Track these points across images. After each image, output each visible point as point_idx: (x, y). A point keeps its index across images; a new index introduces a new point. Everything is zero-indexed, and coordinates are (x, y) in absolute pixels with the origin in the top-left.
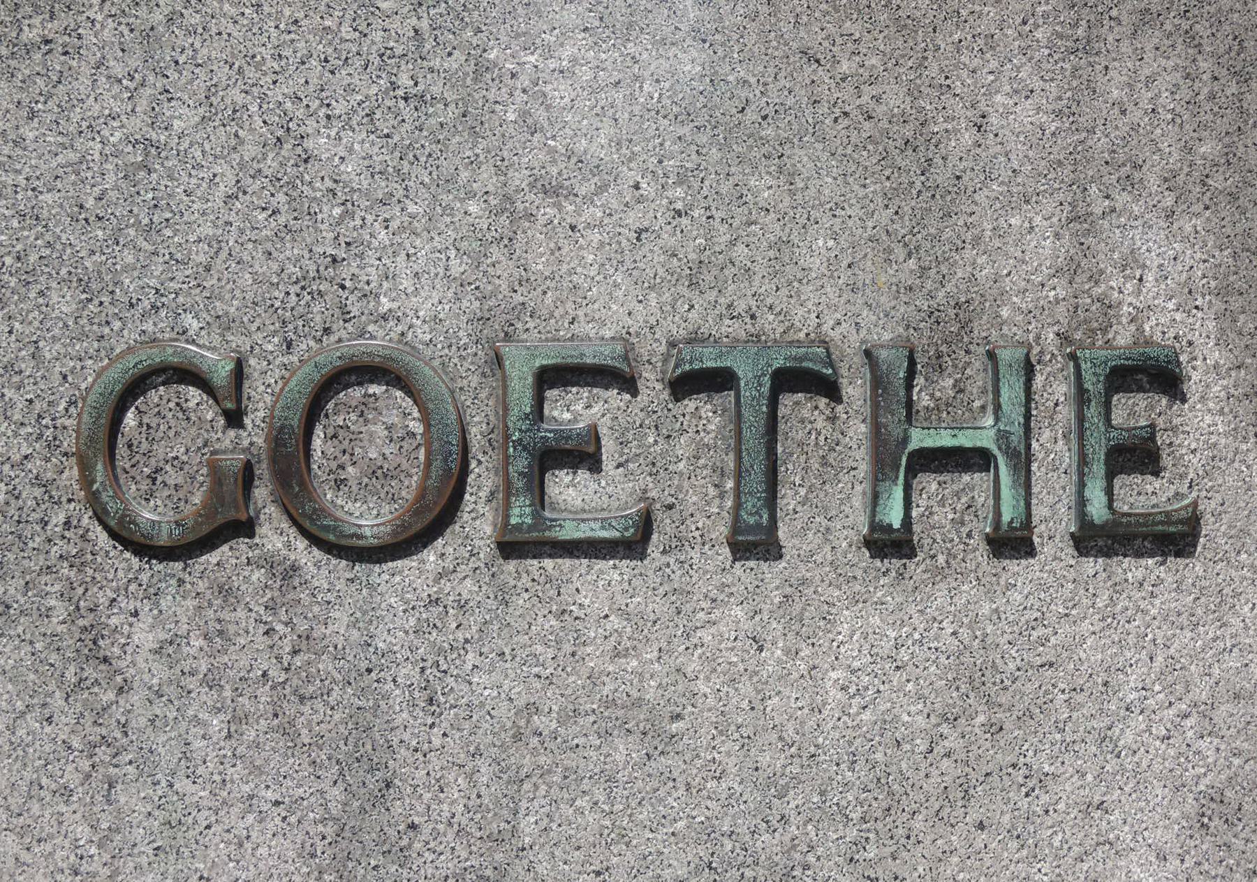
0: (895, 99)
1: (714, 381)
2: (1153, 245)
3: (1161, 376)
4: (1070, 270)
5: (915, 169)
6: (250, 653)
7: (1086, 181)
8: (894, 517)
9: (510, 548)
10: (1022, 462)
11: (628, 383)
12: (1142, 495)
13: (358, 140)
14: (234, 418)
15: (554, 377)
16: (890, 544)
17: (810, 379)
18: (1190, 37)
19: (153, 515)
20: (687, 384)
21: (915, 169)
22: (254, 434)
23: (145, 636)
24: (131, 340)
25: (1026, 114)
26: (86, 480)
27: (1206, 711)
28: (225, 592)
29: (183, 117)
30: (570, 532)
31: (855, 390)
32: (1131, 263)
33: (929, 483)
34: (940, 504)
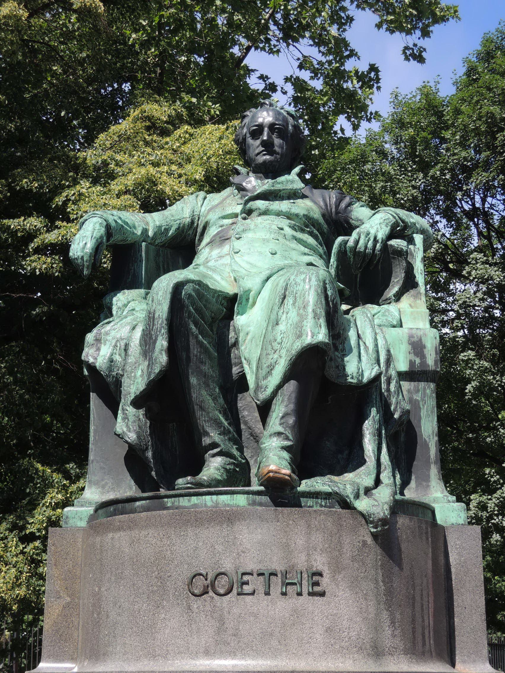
0: (284, 541)
1: (262, 574)
2: (319, 558)
3: (320, 574)
4: (307, 561)
5: (286, 548)
6: (208, 608)
7: (309, 550)
8: (284, 591)
9: (239, 594)
10: (301, 585)
11: (252, 575)
13: (221, 546)
14: (206, 580)
15: (243, 574)
16: (284, 594)
17: (273, 574)
18: (324, 532)
19: (196, 592)
20: (259, 575)
21: (286, 548)
22: (209, 581)
23: (195, 606)
24: (194, 571)
25: (301, 542)
26: (189, 588)
27: (327, 617)
28: (205, 601)
29: (200, 544)
30: (245, 592)
31: (279, 575)
32: (315, 560)
33: (289, 587)
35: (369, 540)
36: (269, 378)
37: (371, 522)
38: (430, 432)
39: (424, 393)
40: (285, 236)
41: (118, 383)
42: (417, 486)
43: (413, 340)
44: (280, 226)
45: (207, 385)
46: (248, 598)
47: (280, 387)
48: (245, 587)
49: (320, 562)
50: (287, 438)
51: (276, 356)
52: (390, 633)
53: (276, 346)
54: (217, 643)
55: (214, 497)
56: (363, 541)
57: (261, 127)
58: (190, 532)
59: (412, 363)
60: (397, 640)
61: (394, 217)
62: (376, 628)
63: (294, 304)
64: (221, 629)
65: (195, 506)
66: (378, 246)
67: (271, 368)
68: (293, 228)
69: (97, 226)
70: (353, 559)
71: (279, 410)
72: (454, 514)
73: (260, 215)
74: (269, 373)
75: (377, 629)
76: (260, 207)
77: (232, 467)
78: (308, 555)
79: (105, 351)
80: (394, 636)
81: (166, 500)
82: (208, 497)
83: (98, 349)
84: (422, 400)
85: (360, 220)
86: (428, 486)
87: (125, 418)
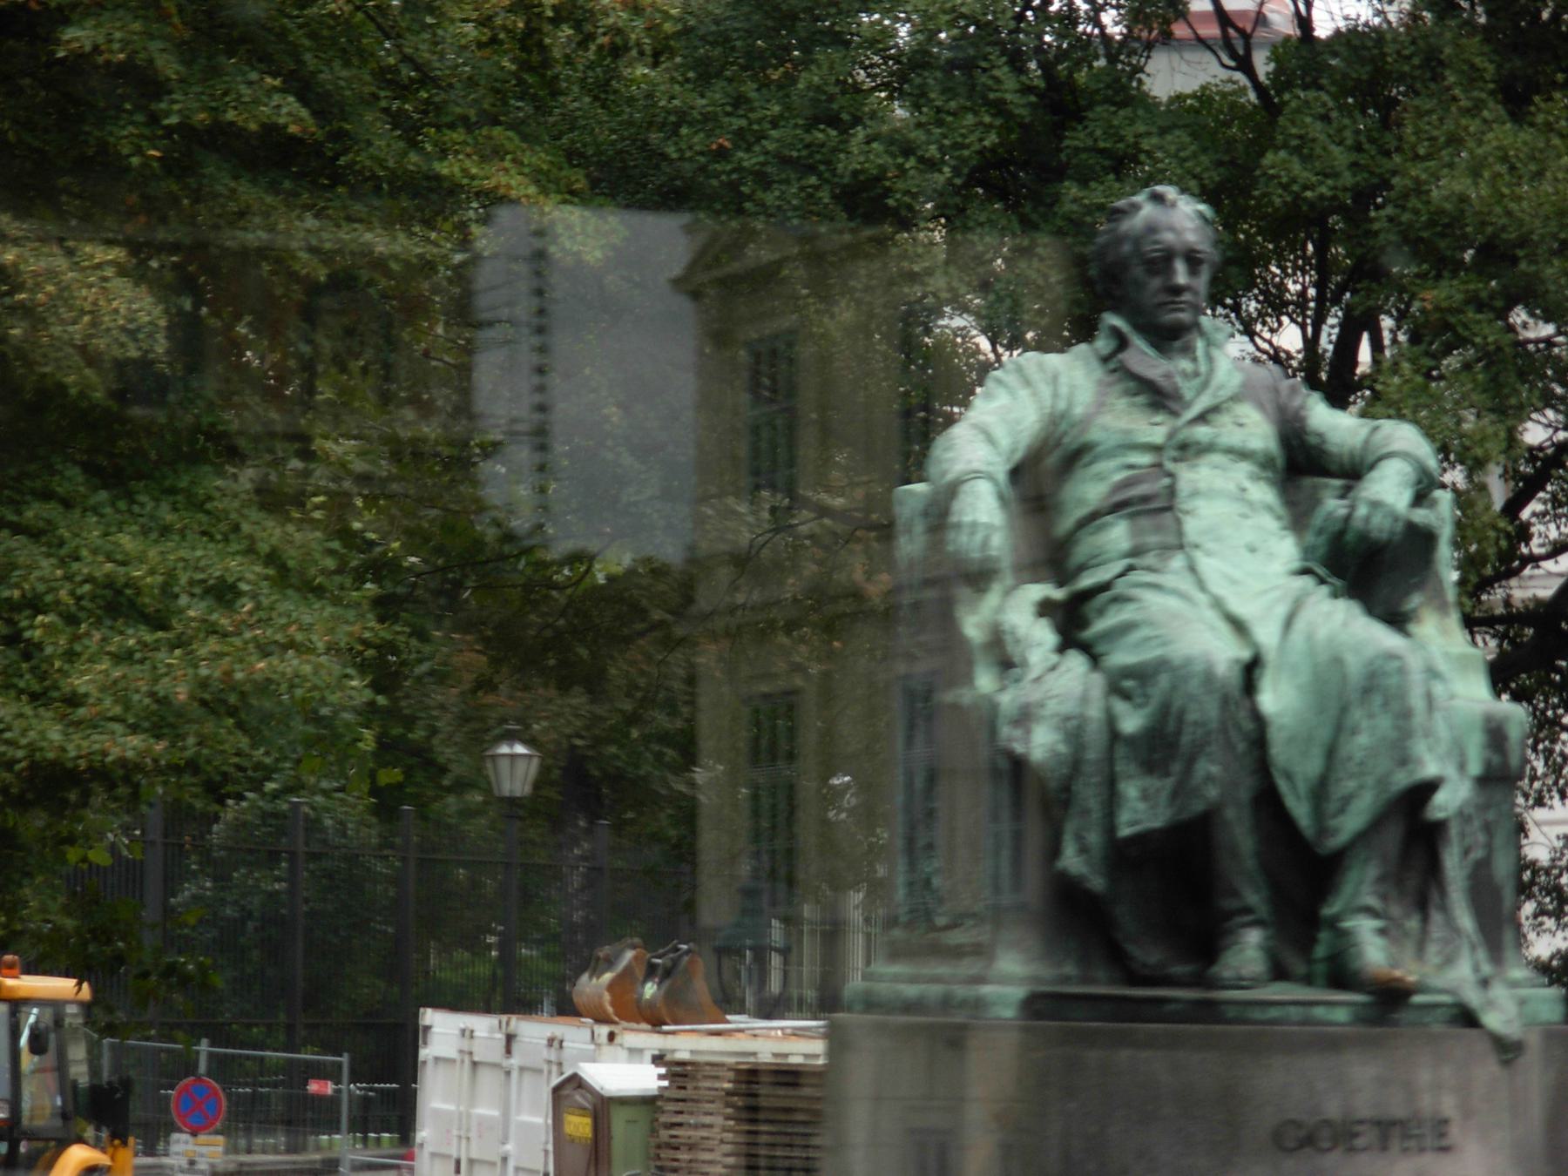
3: (1445, 1122)
12: (1444, 1143)
34: (1412, 1143)
47: (1363, 837)
48: (1360, 1142)
49: (1448, 1105)
57: (1168, 256)
59: (1488, 765)
63: (1385, 704)
66: (1399, 527)
67: (1347, 800)
74: (1342, 810)
83: (1028, 732)
87: (1083, 850)
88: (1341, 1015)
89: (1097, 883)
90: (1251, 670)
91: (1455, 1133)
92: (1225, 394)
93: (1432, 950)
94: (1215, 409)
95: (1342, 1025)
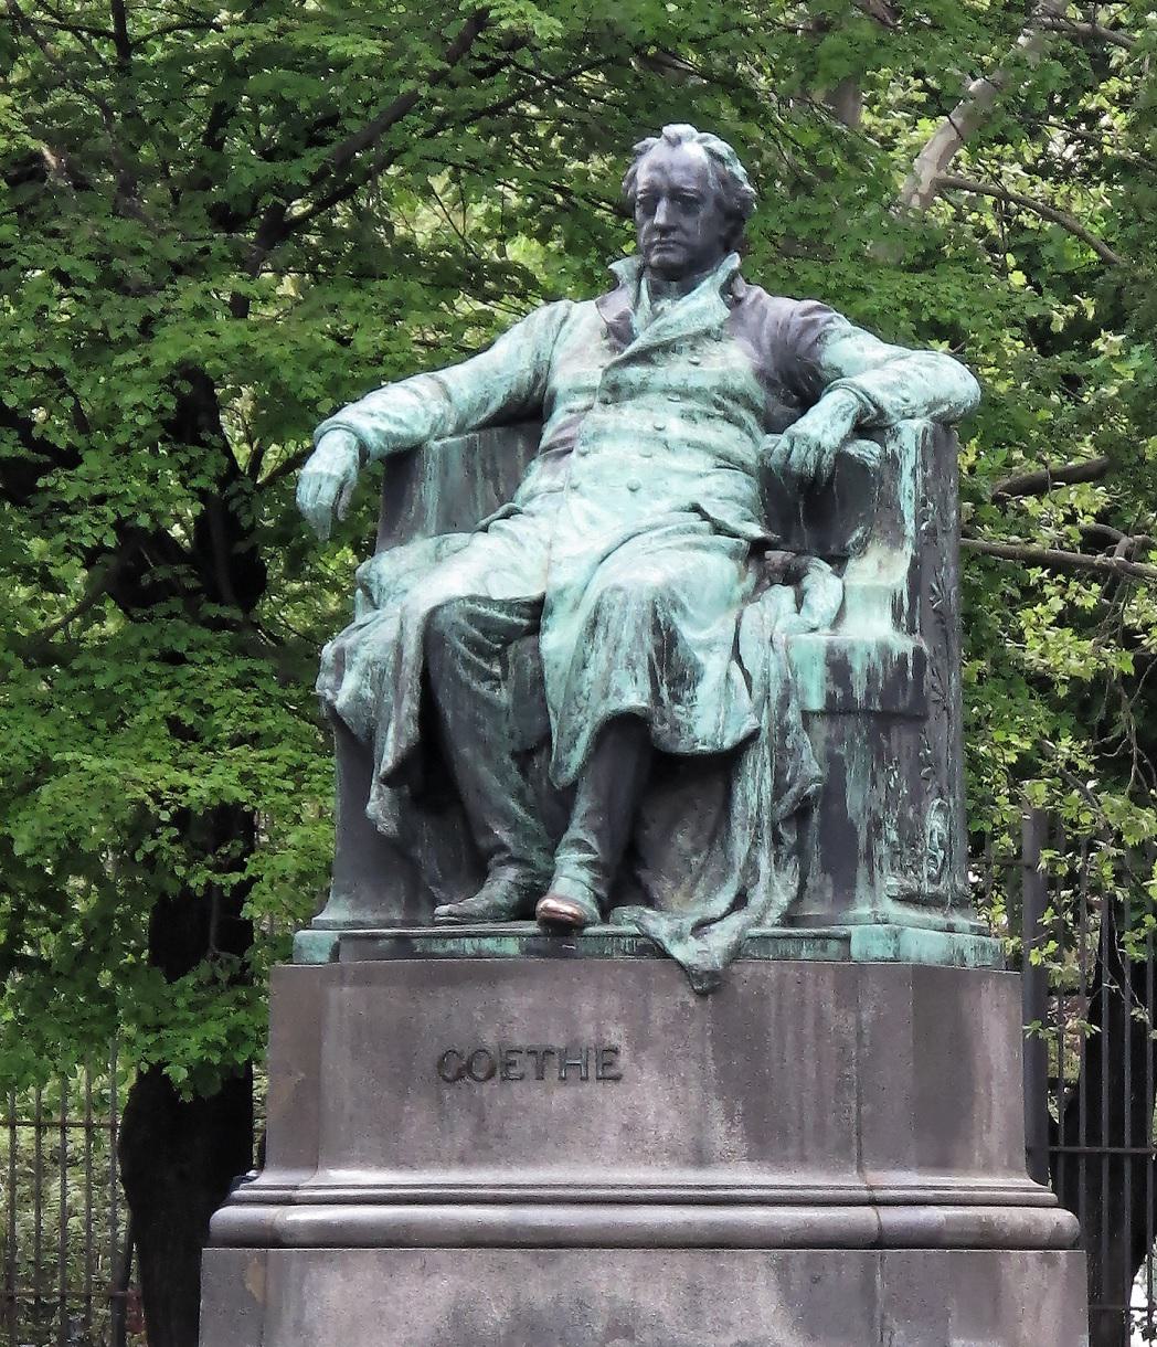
1: (535, 1052)
3: (615, 1051)
5: (569, 1019)
7: (599, 1019)
9: (504, 1079)
12: (612, 1072)
14: (461, 1058)
17: (549, 1052)
19: (449, 1076)
32: (609, 1033)
34: (571, 1073)
35: (692, 1002)
36: (572, 752)
37: (696, 976)
38: (859, 809)
39: (852, 744)
40: (666, 443)
41: (371, 734)
42: (835, 895)
43: (832, 657)
44: (659, 425)
45: (488, 755)
46: (516, 1087)
47: (583, 768)
48: (513, 1071)
49: (615, 1035)
50: (589, 849)
51: (581, 718)
52: (724, 1130)
53: (583, 703)
54: (475, 1146)
55: (476, 941)
56: (682, 1003)
58: (441, 993)
59: (830, 697)
60: (735, 1142)
61: (860, 400)
62: (699, 1124)
63: (605, 638)
64: (481, 1126)
65: (452, 955)
66: (827, 460)
67: (576, 735)
68: (689, 416)
69: (341, 450)
70: (665, 1029)
71: (583, 805)
72: (880, 943)
73: (632, 395)
75: (700, 1125)
76: (633, 381)
77: (528, 881)
78: (599, 1025)
79: (351, 681)
80: (729, 1135)
81: (415, 941)
82: (467, 941)
83: (340, 678)
84: (849, 754)
85: (836, 369)
86: (852, 896)
88: (511, 947)
89: (387, 826)
90: (537, 610)
91: (623, 1060)
92: (669, 335)
93: (702, 884)
94: (667, 348)
95: (514, 957)
